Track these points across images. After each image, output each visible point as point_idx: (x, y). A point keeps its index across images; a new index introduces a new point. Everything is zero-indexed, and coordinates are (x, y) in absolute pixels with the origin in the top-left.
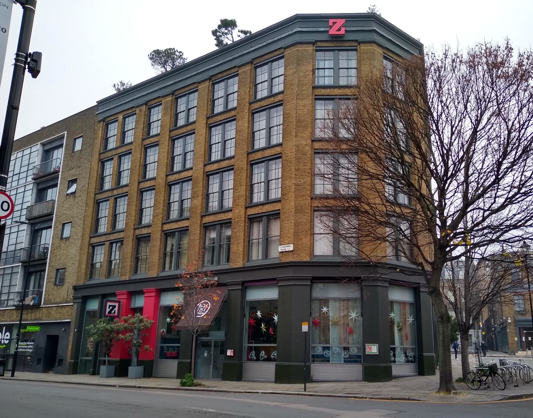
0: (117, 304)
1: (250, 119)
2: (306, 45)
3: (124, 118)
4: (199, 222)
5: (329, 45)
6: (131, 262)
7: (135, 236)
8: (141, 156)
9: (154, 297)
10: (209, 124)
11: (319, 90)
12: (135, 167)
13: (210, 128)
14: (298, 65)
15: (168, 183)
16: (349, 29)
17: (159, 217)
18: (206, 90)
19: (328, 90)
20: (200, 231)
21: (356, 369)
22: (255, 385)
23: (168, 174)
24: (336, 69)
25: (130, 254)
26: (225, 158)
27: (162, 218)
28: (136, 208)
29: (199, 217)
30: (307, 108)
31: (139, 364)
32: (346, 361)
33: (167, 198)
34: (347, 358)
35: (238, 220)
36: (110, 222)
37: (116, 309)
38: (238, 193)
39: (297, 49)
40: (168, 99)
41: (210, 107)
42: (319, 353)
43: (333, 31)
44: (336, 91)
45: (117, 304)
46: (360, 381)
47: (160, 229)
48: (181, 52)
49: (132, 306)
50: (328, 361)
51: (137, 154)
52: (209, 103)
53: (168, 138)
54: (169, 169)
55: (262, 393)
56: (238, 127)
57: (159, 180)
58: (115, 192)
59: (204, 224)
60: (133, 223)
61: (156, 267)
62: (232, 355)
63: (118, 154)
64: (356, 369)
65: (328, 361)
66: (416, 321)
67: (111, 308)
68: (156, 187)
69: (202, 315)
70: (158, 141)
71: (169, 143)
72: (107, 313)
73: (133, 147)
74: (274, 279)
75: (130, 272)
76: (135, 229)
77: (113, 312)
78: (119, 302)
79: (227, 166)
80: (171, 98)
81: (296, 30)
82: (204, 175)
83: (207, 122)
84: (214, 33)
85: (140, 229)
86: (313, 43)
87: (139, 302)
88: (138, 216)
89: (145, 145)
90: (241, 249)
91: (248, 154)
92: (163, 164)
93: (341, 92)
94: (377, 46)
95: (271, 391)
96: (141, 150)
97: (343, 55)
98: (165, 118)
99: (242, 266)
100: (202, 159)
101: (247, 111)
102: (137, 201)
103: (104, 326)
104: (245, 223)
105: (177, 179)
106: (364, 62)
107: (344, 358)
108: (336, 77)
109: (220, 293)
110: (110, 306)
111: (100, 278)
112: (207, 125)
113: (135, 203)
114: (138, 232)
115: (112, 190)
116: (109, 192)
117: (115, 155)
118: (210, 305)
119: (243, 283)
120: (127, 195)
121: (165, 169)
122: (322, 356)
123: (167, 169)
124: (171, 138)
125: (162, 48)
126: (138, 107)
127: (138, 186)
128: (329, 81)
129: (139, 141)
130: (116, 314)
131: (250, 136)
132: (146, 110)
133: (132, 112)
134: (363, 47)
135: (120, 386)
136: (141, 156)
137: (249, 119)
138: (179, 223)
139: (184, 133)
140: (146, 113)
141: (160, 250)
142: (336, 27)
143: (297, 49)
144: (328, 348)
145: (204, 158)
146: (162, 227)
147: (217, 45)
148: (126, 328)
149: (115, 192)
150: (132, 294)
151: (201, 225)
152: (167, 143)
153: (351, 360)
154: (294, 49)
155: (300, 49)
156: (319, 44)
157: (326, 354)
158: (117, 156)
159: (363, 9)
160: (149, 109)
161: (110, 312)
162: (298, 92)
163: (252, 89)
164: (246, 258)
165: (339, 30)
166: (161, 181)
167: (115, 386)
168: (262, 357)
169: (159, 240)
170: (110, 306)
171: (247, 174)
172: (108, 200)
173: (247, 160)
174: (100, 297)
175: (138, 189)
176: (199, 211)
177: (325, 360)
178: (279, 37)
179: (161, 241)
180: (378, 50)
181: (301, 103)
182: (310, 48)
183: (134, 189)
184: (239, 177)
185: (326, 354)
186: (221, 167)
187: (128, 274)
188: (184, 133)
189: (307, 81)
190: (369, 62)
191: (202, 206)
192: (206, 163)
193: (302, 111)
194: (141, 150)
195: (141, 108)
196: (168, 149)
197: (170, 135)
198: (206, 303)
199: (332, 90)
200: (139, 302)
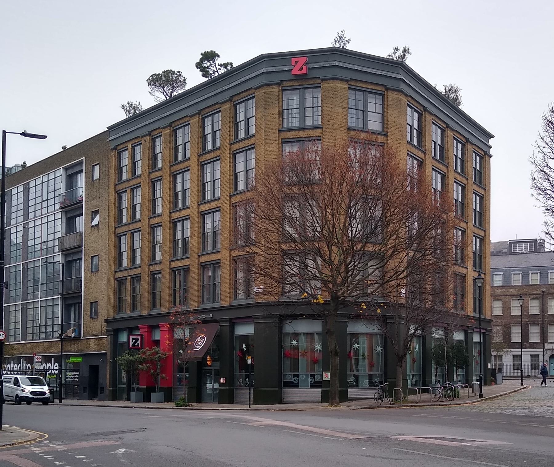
0: (139, 338)
1: (231, 160)
2: (272, 86)
3: (133, 148)
4: (197, 261)
5: (294, 84)
6: (148, 298)
7: (150, 273)
8: (149, 191)
9: (167, 331)
10: (201, 162)
11: (285, 133)
12: (145, 202)
13: (202, 167)
14: (265, 108)
15: (172, 220)
16: (311, 66)
17: (166, 255)
18: (197, 126)
19: (293, 133)
20: (198, 270)
21: (317, 393)
22: (242, 406)
23: (172, 211)
24: (303, 109)
25: (147, 290)
26: (214, 199)
27: (169, 255)
28: (148, 244)
29: (197, 257)
30: (273, 153)
31: (161, 390)
32: (312, 386)
33: (172, 236)
34: (312, 384)
35: (225, 261)
36: (129, 257)
37: (139, 342)
38: (224, 236)
39: (264, 91)
40: (167, 132)
41: (201, 144)
42: (290, 379)
43: (295, 71)
44: (301, 134)
45: (139, 338)
46: (319, 402)
47: (168, 266)
48: (179, 72)
49: (153, 339)
50: (298, 386)
51: (145, 187)
52: (200, 140)
53: (169, 173)
54: (172, 206)
55: (221, 410)
56: (222, 168)
57: (165, 217)
58: (131, 227)
59: (201, 263)
60: (147, 260)
61: (167, 303)
62: (224, 382)
63: (131, 186)
64: (317, 393)
65: (298, 386)
66: (384, 350)
67: (134, 341)
68: (163, 224)
69: (199, 348)
70: (161, 176)
71: (170, 179)
72: (131, 346)
73: (142, 181)
74: (251, 317)
75: (148, 307)
76: (149, 265)
77: (136, 344)
78: (141, 335)
79: (216, 207)
80: (169, 131)
81: (262, 71)
82: (198, 215)
83: (198, 160)
84: (199, 65)
85: (153, 266)
86: (279, 84)
87: (157, 335)
88: (151, 253)
89: (152, 179)
90: (228, 289)
91: (231, 196)
92: (166, 201)
93: (305, 133)
94: (339, 82)
95: (211, 409)
96: (149, 184)
97: (308, 94)
98: (166, 152)
99: (229, 305)
100: (196, 199)
101: (228, 152)
102: (149, 237)
103: (128, 358)
104: (230, 264)
105: (179, 217)
106: (327, 101)
107: (310, 384)
108: (303, 117)
109: (205, 330)
110: (133, 339)
111: (127, 313)
112: (198, 163)
113: (147, 240)
114: (152, 268)
115: (128, 224)
116: (126, 226)
117: (128, 187)
118: (205, 337)
119: (230, 320)
120: (140, 231)
121: (168, 206)
122: (292, 382)
123: (170, 206)
124: (172, 173)
125: (160, 71)
126: (142, 137)
127: (149, 221)
128: (296, 123)
129: (146, 175)
130: (140, 346)
131: (232, 178)
132: (150, 140)
133: (139, 142)
134: (325, 85)
135: (132, 407)
136: (149, 191)
137: (230, 160)
138: (183, 261)
139: (182, 169)
140: (151, 144)
141: (169, 286)
142: (299, 66)
143: (264, 91)
144: (297, 376)
145: (198, 198)
146: (170, 264)
147: (203, 75)
148: (143, 359)
149: (131, 227)
150: (152, 328)
151: (198, 264)
152: (168, 179)
153: (315, 385)
154: (262, 91)
155: (266, 91)
156: (285, 84)
157: (295, 380)
158: (129, 189)
159: (327, 43)
160: (152, 139)
161: (133, 345)
162: (266, 137)
163: (231, 129)
164: (233, 297)
165: (301, 69)
166: (166, 218)
167: (132, 407)
168: (247, 384)
169: (168, 277)
170: (133, 339)
171: (230, 217)
172: (126, 234)
173: (230, 203)
174: (128, 330)
175: (149, 225)
176: (197, 251)
177: (295, 385)
178: (247, 78)
179: (169, 278)
180: (341, 85)
181: (269, 148)
182: (276, 89)
183: (145, 225)
184: (224, 219)
185: (295, 380)
186: (211, 208)
187: (147, 309)
188: (182, 169)
189: (274, 125)
190: (330, 100)
191: (198, 245)
192: (200, 203)
193: (269, 156)
194: (149, 184)
195: (145, 138)
196: (170, 185)
197: (170, 170)
198: (203, 338)
199: (297, 132)
200: (157, 335)
